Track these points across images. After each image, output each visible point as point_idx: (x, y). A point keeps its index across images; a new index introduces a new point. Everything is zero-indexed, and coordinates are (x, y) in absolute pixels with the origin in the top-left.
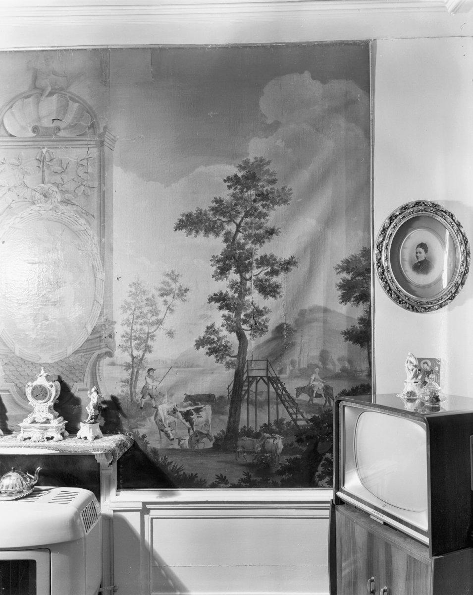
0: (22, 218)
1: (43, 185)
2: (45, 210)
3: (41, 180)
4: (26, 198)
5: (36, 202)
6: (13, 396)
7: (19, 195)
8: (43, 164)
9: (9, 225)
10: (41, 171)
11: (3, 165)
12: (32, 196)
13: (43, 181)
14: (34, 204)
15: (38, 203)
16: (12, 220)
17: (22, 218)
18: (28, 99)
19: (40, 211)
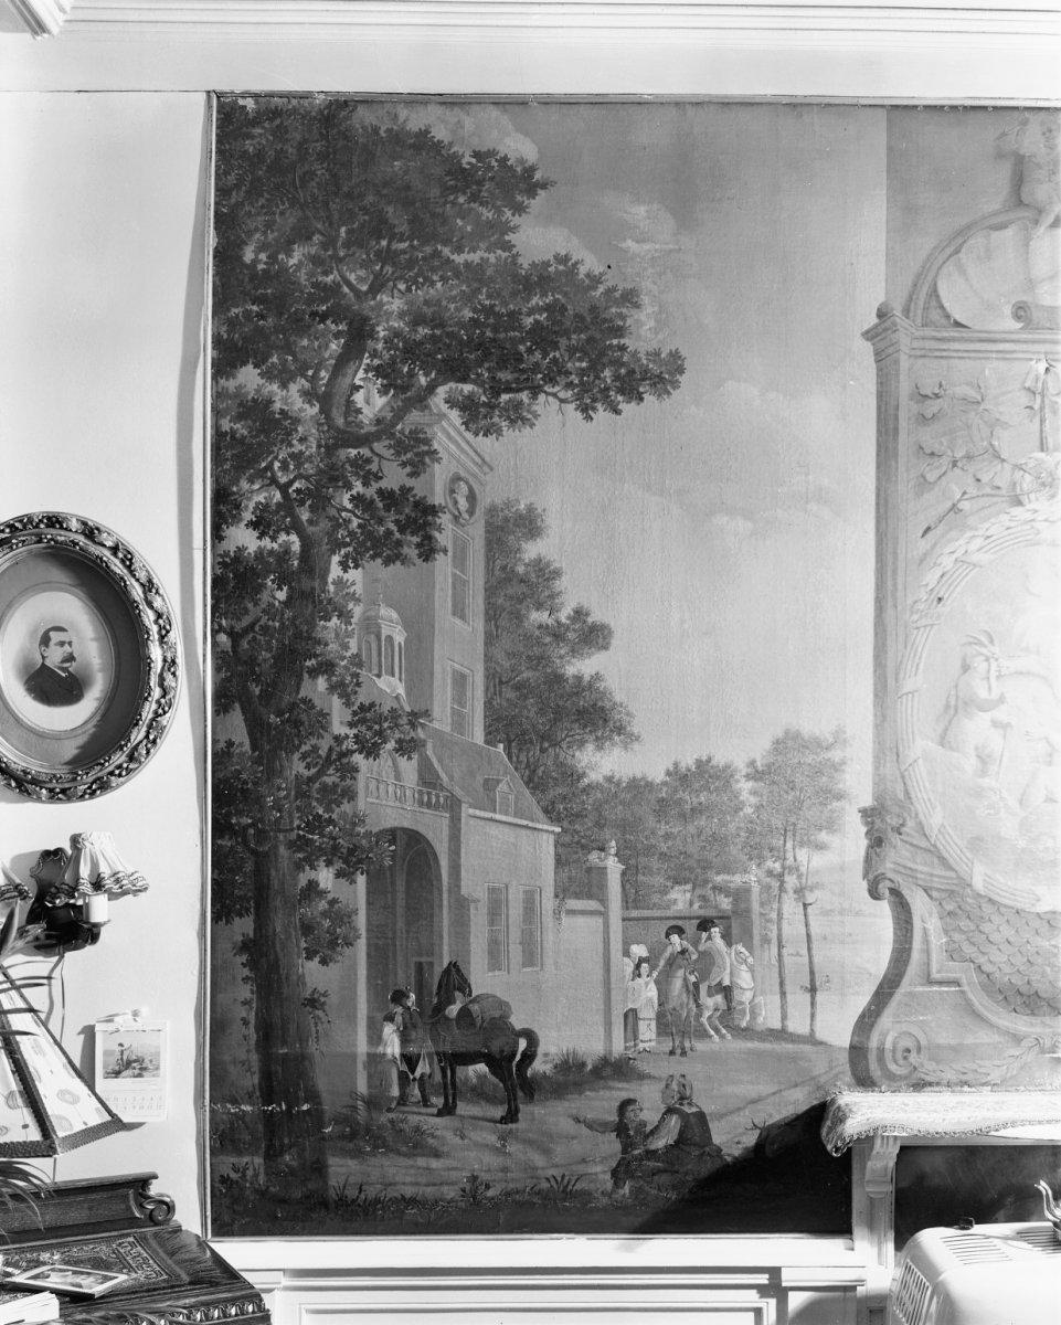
0: (988, 537)
1: (1042, 455)
2: (1046, 520)
3: (1038, 444)
4: (999, 488)
5: (1024, 499)
6: (970, 996)
7: (979, 480)
8: (1043, 401)
9: (955, 556)
10: (1037, 420)
11: (939, 401)
12: (1015, 484)
13: (1042, 444)
14: (1020, 503)
15: (1030, 502)
16: (961, 542)
17: (988, 537)
18: (997, 233)
19: (1033, 520)
